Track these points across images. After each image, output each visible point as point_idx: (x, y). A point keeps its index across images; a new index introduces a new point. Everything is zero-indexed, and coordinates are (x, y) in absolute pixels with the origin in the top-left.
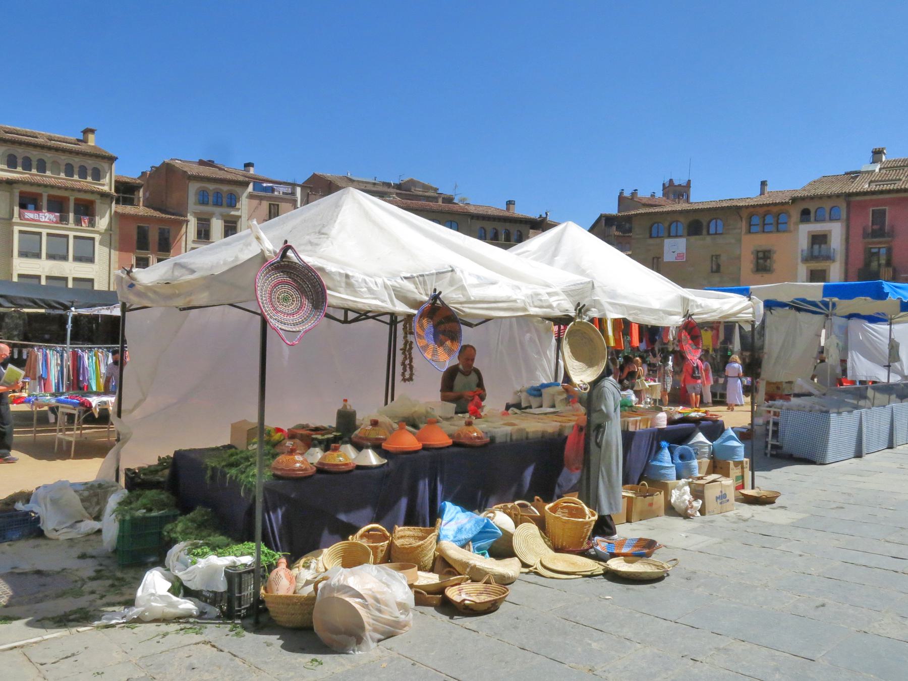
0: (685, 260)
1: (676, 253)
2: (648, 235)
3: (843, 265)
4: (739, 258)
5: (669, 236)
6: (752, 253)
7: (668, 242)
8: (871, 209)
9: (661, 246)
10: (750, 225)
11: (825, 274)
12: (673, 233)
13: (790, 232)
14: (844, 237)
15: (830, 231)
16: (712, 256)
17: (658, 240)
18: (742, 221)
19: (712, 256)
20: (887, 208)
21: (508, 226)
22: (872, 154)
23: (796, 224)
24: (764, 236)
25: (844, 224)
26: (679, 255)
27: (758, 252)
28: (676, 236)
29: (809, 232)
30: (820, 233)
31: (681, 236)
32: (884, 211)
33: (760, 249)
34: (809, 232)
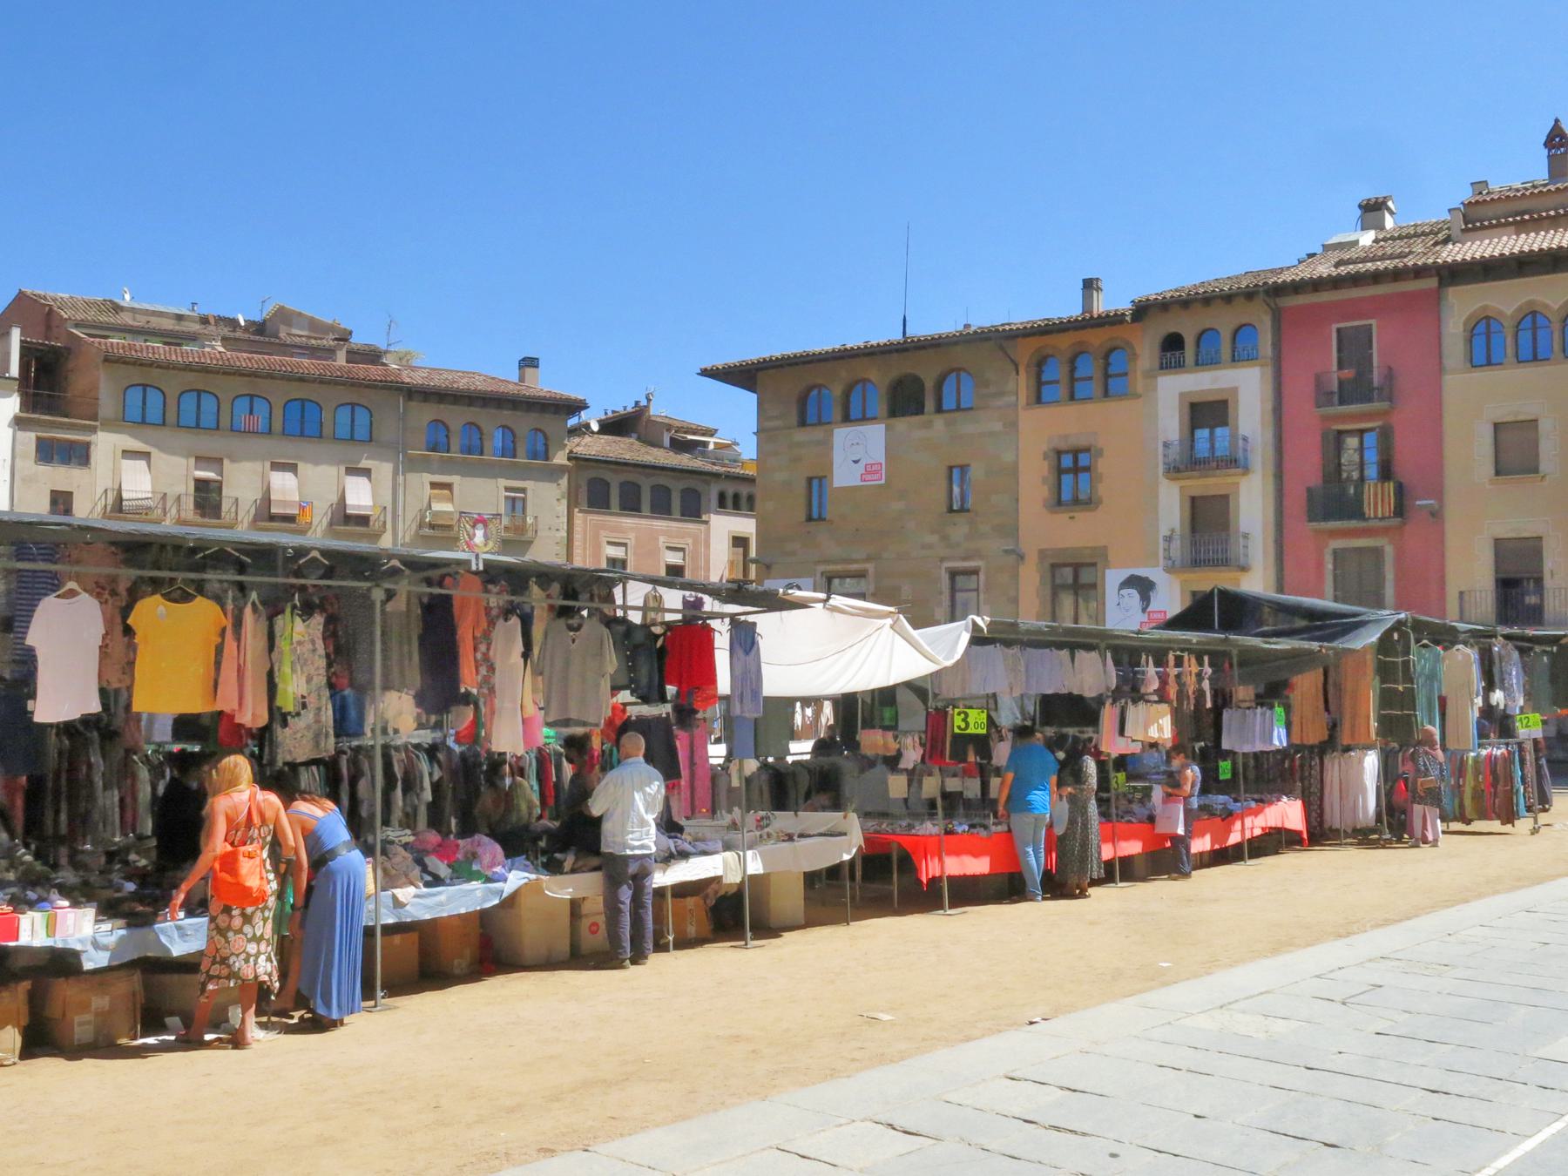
0: (883, 482)
1: (862, 465)
2: (794, 419)
3: (1271, 481)
4: (1014, 471)
5: (847, 419)
6: (1046, 457)
7: (843, 436)
8: (1334, 327)
9: (826, 445)
10: (1040, 384)
11: (1228, 503)
12: (855, 411)
13: (1137, 396)
14: (1269, 406)
15: (1234, 391)
16: (951, 468)
17: (817, 434)
18: (1017, 373)
19: (951, 468)
20: (1373, 322)
21: (506, 416)
22: (1359, 212)
23: (1150, 375)
24: (1072, 410)
25: (1269, 371)
26: (870, 470)
27: (1059, 453)
28: (864, 419)
29: (1182, 395)
30: (1211, 398)
31: (874, 419)
32: (1369, 328)
33: (1063, 446)
34: (1182, 395)
